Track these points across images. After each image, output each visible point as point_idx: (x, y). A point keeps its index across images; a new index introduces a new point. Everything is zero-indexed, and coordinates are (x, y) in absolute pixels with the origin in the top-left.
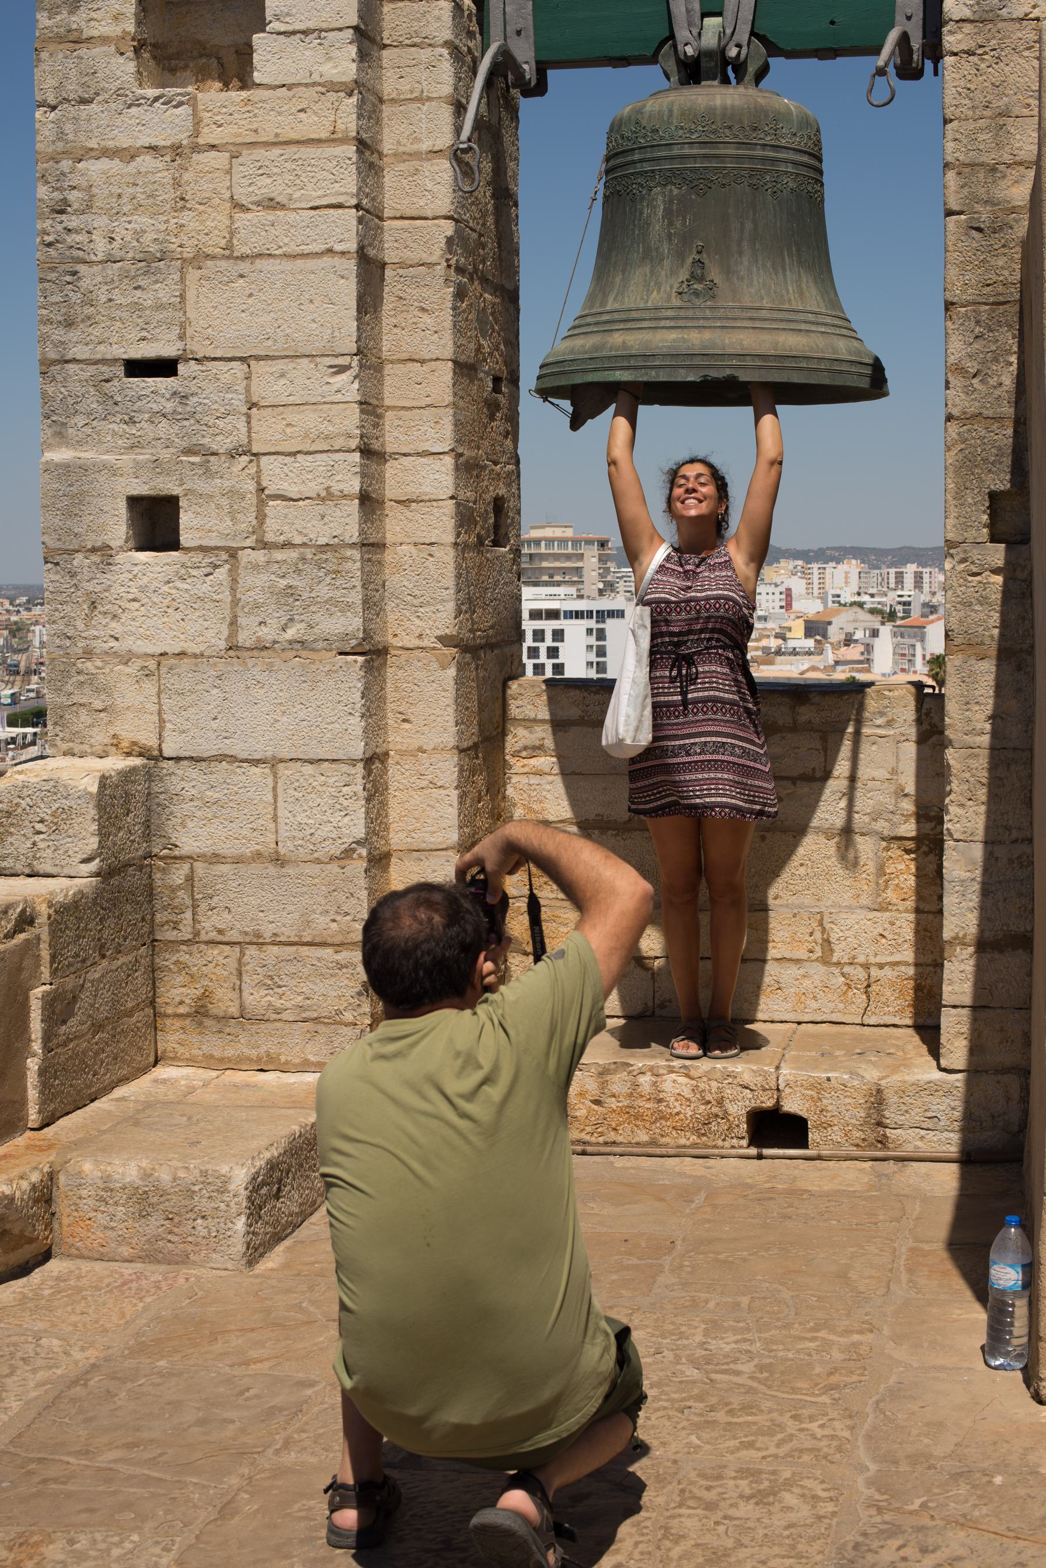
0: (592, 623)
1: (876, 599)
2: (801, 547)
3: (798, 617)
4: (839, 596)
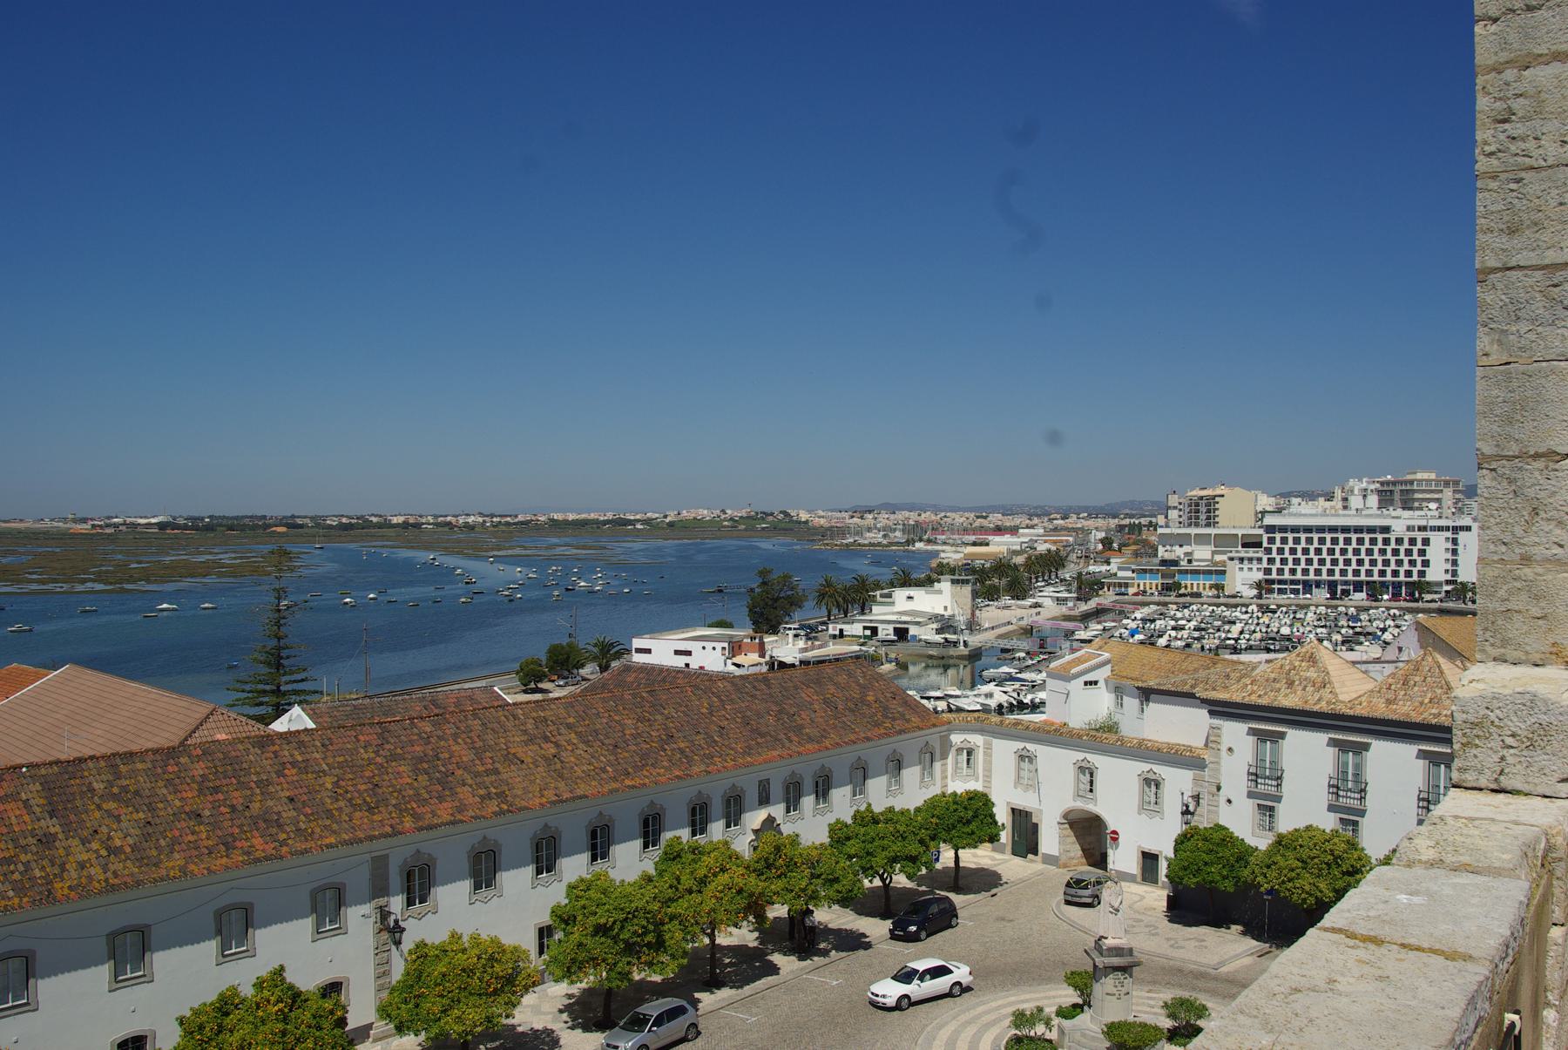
0: (1449, 534)
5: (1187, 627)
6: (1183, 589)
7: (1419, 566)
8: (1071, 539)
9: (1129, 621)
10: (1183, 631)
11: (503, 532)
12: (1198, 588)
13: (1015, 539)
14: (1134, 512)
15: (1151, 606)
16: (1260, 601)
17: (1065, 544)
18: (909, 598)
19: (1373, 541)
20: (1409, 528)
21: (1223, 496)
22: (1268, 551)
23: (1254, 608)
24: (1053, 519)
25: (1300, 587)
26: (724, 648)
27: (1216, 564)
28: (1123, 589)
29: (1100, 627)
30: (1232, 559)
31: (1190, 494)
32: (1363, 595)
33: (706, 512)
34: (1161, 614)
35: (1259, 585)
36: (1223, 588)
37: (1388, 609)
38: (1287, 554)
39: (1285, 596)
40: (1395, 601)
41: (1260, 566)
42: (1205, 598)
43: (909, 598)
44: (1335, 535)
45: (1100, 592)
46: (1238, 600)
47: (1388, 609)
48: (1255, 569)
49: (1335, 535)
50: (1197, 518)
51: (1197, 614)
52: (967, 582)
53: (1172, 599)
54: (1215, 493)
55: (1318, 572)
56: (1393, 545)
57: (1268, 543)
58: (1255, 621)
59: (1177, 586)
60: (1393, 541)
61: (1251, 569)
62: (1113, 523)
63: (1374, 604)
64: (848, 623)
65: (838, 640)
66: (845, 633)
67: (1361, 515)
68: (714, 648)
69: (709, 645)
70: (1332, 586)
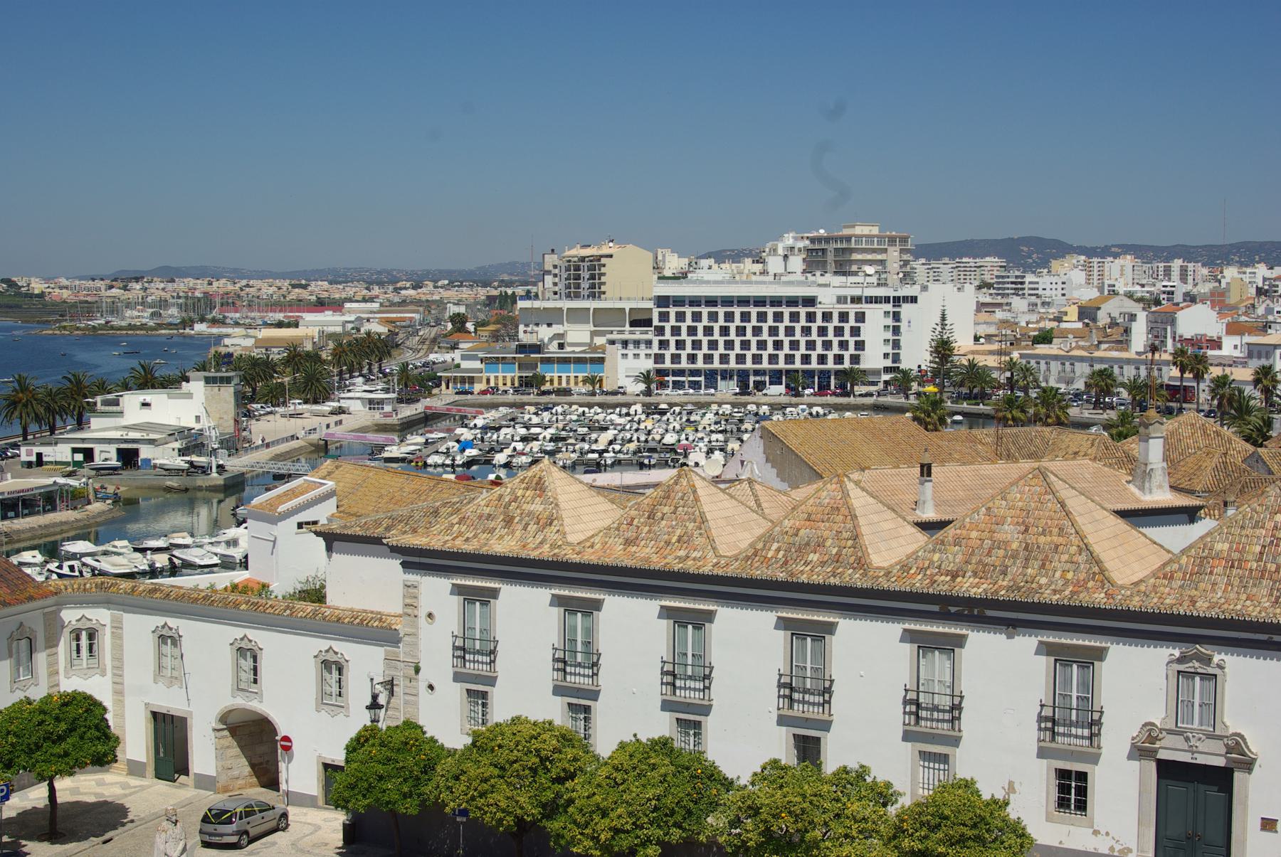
0: (889, 307)
1: (1146, 289)
2: (1088, 244)
3: (1074, 304)
4: (1114, 286)
5: (541, 437)
6: (548, 384)
7: (852, 350)
8: (416, 316)
9: (464, 430)
10: (535, 442)
12: (568, 382)
14: (514, 278)
15: (501, 409)
16: (648, 399)
17: (408, 323)
19: (795, 317)
20: (841, 300)
21: (611, 256)
22: (660, 331)
23: (638, 408)
24: (401, 289)
25: (702, 379)
27: (594, 348)
28: (467, 386)
29: (421, 440)
30: (612, 342)
31: (567, 253)
32: (781, 389)
34: (513, 420)
35: (646, 378)
36: (601, 381)
37: (810, 406)
38: (684, 336)
39: (681, 392)
40: (820, 395)
41: (649, 352)
42: (575, 396)
44: (745, 309)
45: (435, 391)
46: (619, 398)
47: (810, 406)
49: (745, 309)
50: (578, 286)
51: (561, 417)
52: (228, 380)
53: (532, 398)
55: (724, 358)
56: (819, 322)
57: (660, 321)
58: (635, 426)
59: (542, 380)
60: (819, 317)
62: (482, 293)
63: (794, 400)
64: (49, 444)
65: (35, 470)
66: (45, 459)
67: (779, 283)
70: (743, 376)
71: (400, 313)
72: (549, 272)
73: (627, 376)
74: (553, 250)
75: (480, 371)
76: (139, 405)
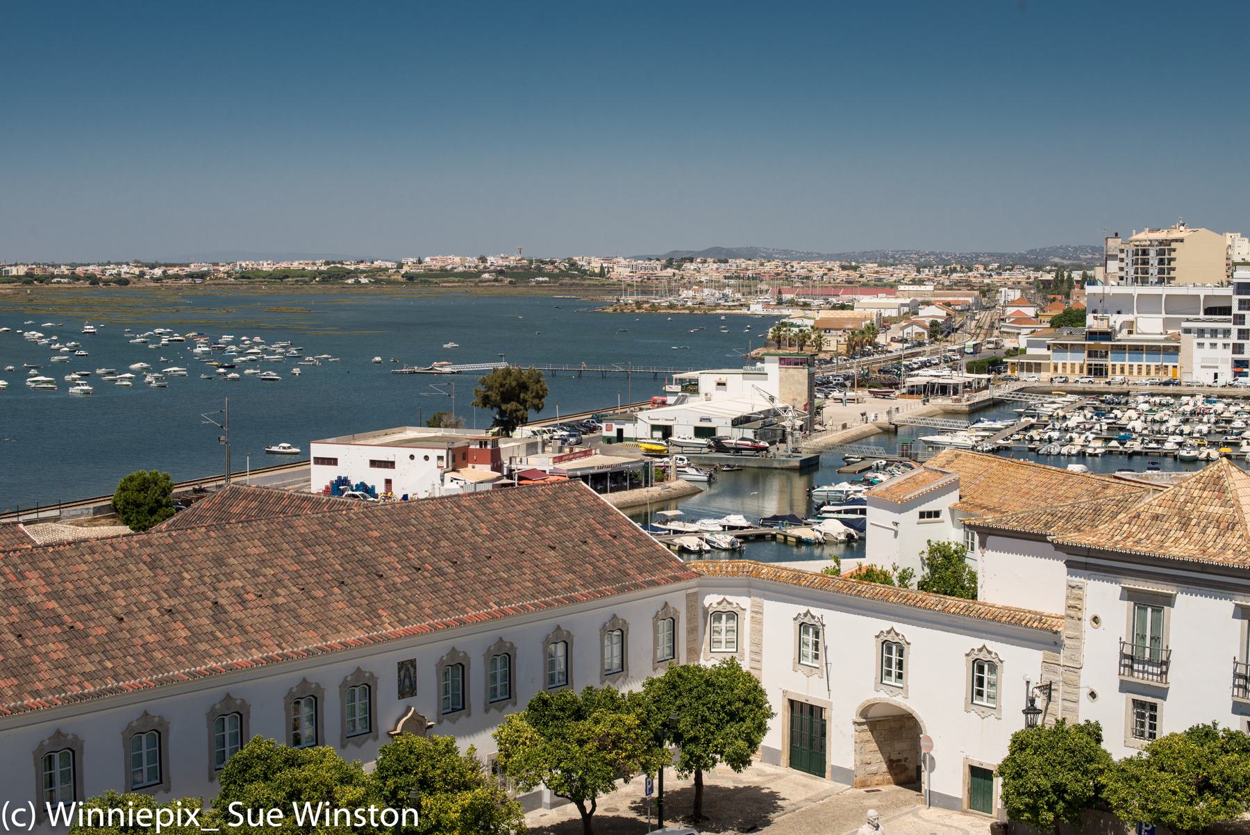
11: (168, 288)
13: (893, 301)
14: (1066, 262)
18: (719, 384)
21: (1182, 241)
26: (440, 458)
30: (1188, 331)
31: (1135, 237)
33: (457, 259)
41: (1226, 341)
43: (719, 384)
48: (1220, 346)
54: (1171, 237)
57: (1240, 309)
61: (1203, 344)
68: (426, 458)
69: (419, 453)
71: (954, 296)
72: (1114, 257)
73: (1202, 367)
74: (1116, 234)
75: (1048, 357)
76: (715, 384)
